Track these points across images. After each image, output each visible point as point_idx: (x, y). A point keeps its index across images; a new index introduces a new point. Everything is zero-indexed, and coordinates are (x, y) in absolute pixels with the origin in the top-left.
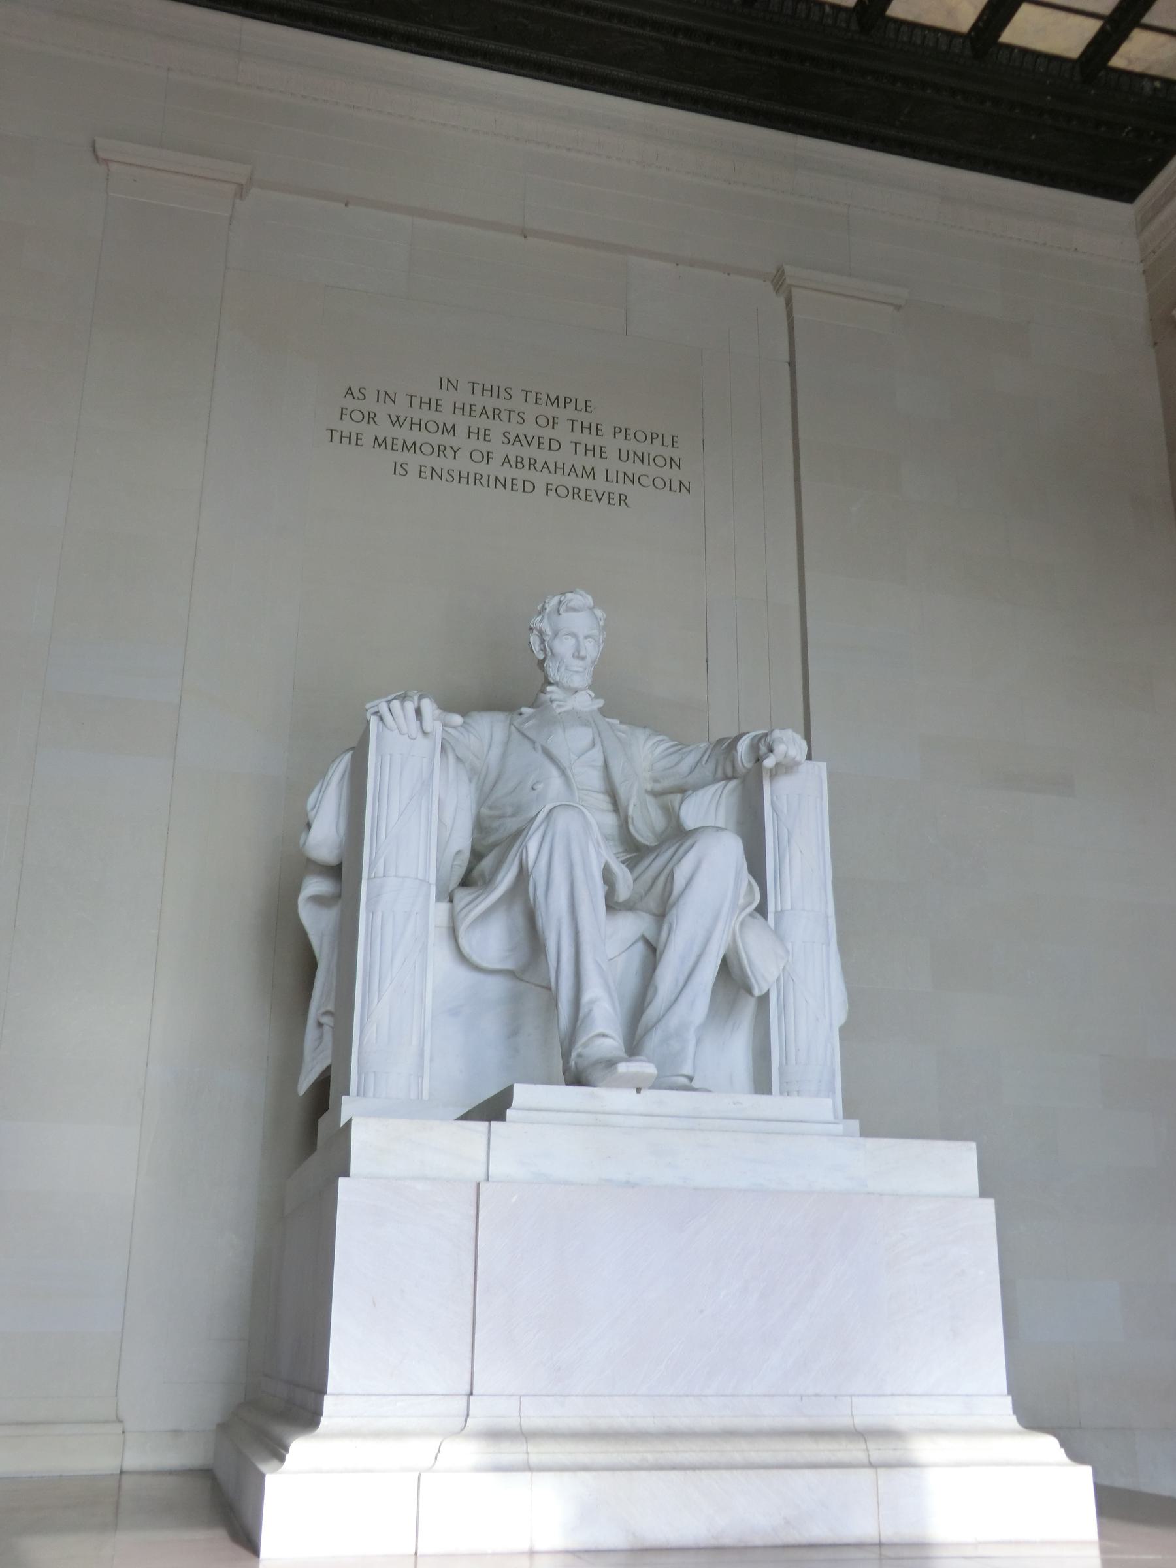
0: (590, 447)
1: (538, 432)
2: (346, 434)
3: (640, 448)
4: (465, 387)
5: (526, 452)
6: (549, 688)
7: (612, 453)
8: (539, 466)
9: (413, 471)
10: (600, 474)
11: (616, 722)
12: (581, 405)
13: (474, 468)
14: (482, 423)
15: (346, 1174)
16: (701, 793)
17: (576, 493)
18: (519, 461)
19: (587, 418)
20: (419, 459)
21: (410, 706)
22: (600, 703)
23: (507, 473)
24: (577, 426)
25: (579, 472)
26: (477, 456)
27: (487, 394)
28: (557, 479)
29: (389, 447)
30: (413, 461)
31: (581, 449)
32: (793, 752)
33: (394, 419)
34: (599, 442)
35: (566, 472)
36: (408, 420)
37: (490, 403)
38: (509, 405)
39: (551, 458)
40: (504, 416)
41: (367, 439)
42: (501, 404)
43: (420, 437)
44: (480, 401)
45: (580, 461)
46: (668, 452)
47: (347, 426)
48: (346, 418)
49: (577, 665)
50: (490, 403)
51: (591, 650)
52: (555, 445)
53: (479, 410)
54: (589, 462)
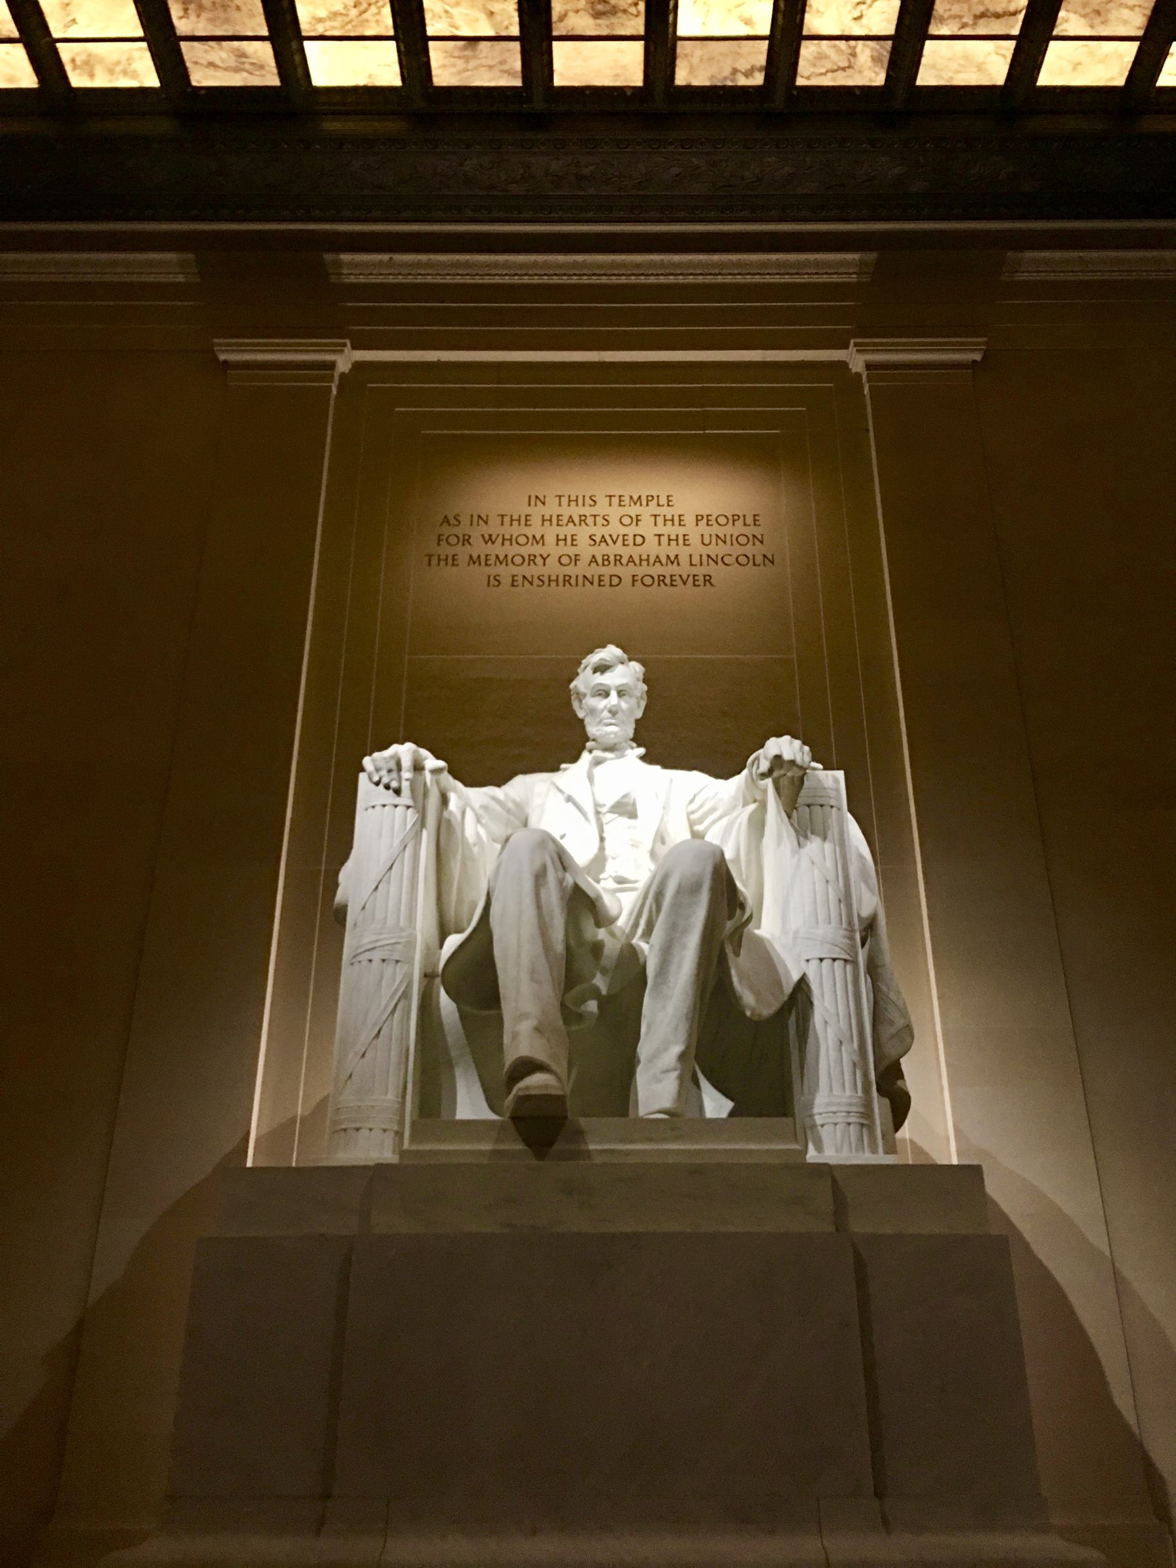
0: (673, 537)
1: (623, 530)
2: (443, 557)
3: (722, 532)
4: (552, 501)
5: (612, 550)
6: (589, 744)
7: (694, 539)
8: (624, 561)
9: (506, 581)
10: (684, 560)
12: (663, 501)
14: (570, 529)
16: (725, 821)
18: (606, 559)
20: (513, 570)
22: (642, 751)
24: (660, 520)
25: (664, 561)
26: (565, 560)
27: (573, 504)
29: (483, 563)
30: (505, 572)
31: (664, 540)
33: (487, 537)
34: (681, 531)
35: (652, 561)
36: (500, 538)
37: (576, 511)
38: (594, 511)
39: (636, 552)
40: (590, 520)
41: (463, 559)
42: (587, 511)
43: (512, 550)
44: (566, 511)
45: (664, 551)
46: (749, 531)
47: (445, 550)
48: (443, 543)
50: (576, 511)
52: (639, 540)
53: (565, 519)
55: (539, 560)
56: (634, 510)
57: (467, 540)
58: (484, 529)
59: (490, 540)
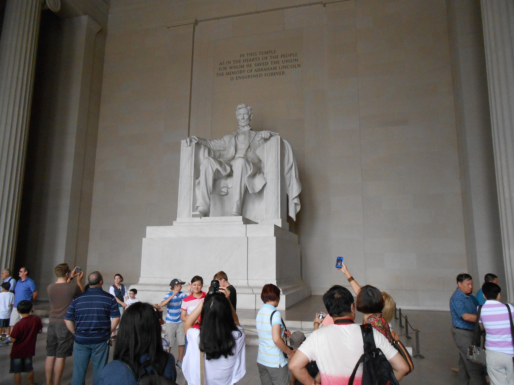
5: (260, 67)
9: (235, 78)
10: (278, 68)
11: (253, 132)
12: (273, 52)
13: (248, 74)
15: (145, 237)
17: (272, 74)
18: (258, 69)
19: (274, 55)
21: (185, 141)
22: (250, 128)
23: (256, 73)
26: (249, 71)
28: (267, 72)
30: (235, 76)
31: (273, 63)
32: (263, 136)
38: (256, 57)
39: (265, 67)
40: (255, 60)
41: (225, 74)
46: (294, 58)
47: (221, 72)
49: (242, 121)
50: (251, 57)
51: (246, 117)
54: (275, 66)
55: (243, 72)
56: (265, 56)
57: (225, 68)
58: (230, 65)
59: (231, 68)
